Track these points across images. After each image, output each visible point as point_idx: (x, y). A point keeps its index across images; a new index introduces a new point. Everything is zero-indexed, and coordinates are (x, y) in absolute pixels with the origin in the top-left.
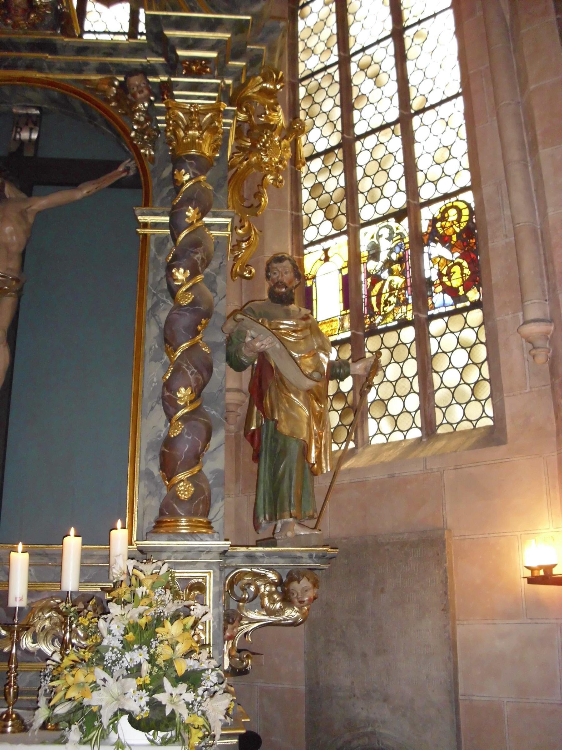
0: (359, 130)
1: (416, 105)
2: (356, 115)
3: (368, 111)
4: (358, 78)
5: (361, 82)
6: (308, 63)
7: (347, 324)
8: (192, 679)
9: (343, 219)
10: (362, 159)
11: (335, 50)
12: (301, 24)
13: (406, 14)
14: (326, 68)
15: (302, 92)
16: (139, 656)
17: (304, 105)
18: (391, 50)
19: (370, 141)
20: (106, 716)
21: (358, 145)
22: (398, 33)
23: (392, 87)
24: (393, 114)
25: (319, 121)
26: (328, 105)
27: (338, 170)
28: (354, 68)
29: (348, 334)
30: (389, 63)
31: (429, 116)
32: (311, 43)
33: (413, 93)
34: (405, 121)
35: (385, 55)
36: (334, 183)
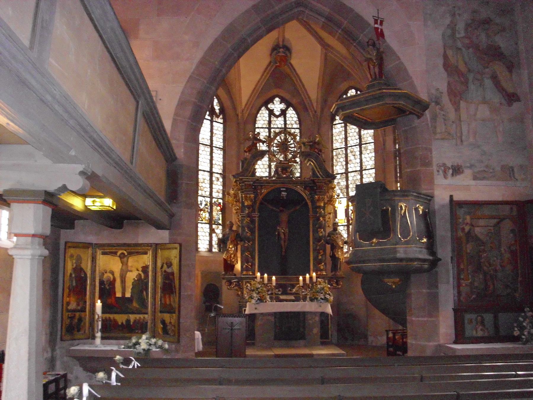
0: (350, 170)
1: (364, 168)
2: (349, 166)
3: (352, 165)
4: (350, 155)
5: (351, 157)
6: (336, 145)
7: (346, 221)
8: (329, 294)
9: (345, 194)
10: (350, 178)
11: (344, 143)
12: (334, 131)
13: (363, 140)
14: (341, 148)
15: (334, 153)
16: (322, 291)
17: (335, 158)
18: (358, 149)
19: (353, 174)
20: (319, 298)
21: (349, 174)
22: (360, 145)
23: (358, 161)
24: (358, 169)
25: (339, 164)
26: (342, 160)
27: (344, 180)
28: (349, 151)
29: (346, 224)
30: (358, 153)
31: (367, 172)
32: (337, 138)
33: (363, 164)
34: (361, 171)
35: (357, 149)
36: (343, 183)
